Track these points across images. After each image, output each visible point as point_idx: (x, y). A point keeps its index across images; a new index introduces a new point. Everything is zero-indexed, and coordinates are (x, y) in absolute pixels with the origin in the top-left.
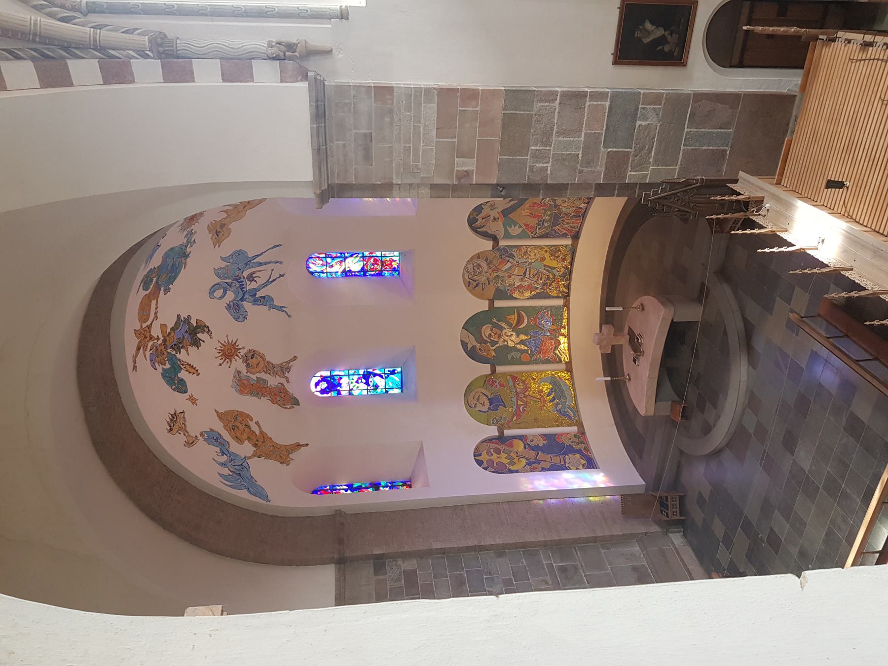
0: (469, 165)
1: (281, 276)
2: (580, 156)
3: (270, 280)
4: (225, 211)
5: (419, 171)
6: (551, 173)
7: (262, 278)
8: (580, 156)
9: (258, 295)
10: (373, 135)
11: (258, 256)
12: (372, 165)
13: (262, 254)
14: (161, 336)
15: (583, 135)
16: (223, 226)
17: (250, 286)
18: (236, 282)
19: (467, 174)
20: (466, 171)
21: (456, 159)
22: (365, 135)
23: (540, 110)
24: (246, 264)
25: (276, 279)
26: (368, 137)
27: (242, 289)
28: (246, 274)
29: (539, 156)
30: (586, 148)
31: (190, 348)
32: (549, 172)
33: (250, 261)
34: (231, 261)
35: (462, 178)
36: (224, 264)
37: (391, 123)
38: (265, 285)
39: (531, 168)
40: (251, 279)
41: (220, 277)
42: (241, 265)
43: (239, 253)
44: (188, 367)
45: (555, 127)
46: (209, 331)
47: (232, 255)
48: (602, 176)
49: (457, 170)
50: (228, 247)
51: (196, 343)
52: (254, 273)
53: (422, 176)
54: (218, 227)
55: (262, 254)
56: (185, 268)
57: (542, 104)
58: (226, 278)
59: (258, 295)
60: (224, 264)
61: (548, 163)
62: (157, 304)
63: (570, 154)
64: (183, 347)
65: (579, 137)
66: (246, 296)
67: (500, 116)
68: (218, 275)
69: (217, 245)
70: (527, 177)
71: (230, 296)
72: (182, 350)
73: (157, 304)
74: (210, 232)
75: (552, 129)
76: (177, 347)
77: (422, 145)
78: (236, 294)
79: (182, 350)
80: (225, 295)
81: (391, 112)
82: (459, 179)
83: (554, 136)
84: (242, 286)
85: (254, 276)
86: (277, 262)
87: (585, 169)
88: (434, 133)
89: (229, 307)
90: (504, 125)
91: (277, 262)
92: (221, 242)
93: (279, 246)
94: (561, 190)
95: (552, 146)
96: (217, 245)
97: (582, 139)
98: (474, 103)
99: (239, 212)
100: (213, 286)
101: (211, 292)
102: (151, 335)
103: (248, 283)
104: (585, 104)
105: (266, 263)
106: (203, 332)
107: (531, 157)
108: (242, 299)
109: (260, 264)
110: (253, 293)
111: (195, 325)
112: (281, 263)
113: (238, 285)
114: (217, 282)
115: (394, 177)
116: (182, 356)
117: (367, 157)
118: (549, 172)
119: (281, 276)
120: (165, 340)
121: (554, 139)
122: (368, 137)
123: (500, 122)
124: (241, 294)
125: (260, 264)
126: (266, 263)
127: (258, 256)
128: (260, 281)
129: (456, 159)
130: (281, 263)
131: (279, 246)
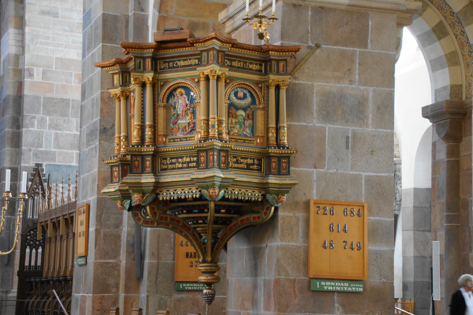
0: (38, 77)
2: (41, 149)
5: (34, 44)
6: (30, 131)
8: (41, 149)
10: (57, 18)
12: (38, 15)
15: (55, 150)
19: (31, 75)
20: (33, 74)
21: (41, 69)
22: (57, 14)
23: (71, 122)
26: (56, 15)
29: (42, 121)
30: (47, 153)
32: (31, 129)
35: (28, 71)
37: (65, 30)
39: (34, 117)
45: (60, 132)
48: (26, 165)
49: (33, 69)
53: (31, 46)
57: (75, 123)
61: (37, 128)
63: (43, 143)
65: (54, 148)
67: (68, 97)
70: (28, 114)
75: (59, 130)
77: (51, 48)
81: (72, 31)
82: (28, 70)
83: (55, 131)
87: (31, 153)
88: (59, 56)
90: (63, 100)
94: (12, 143)
95: (49, 131)
97: (53, 150)
98: (77, 81)
104: (74, 150)
107: (42, 117)
115: (30, 28)
117: (43, 13)
118: (31, 129)
121: (53, 131)
122: (56, 15)
123: (64, 97)
129: (41, 69)
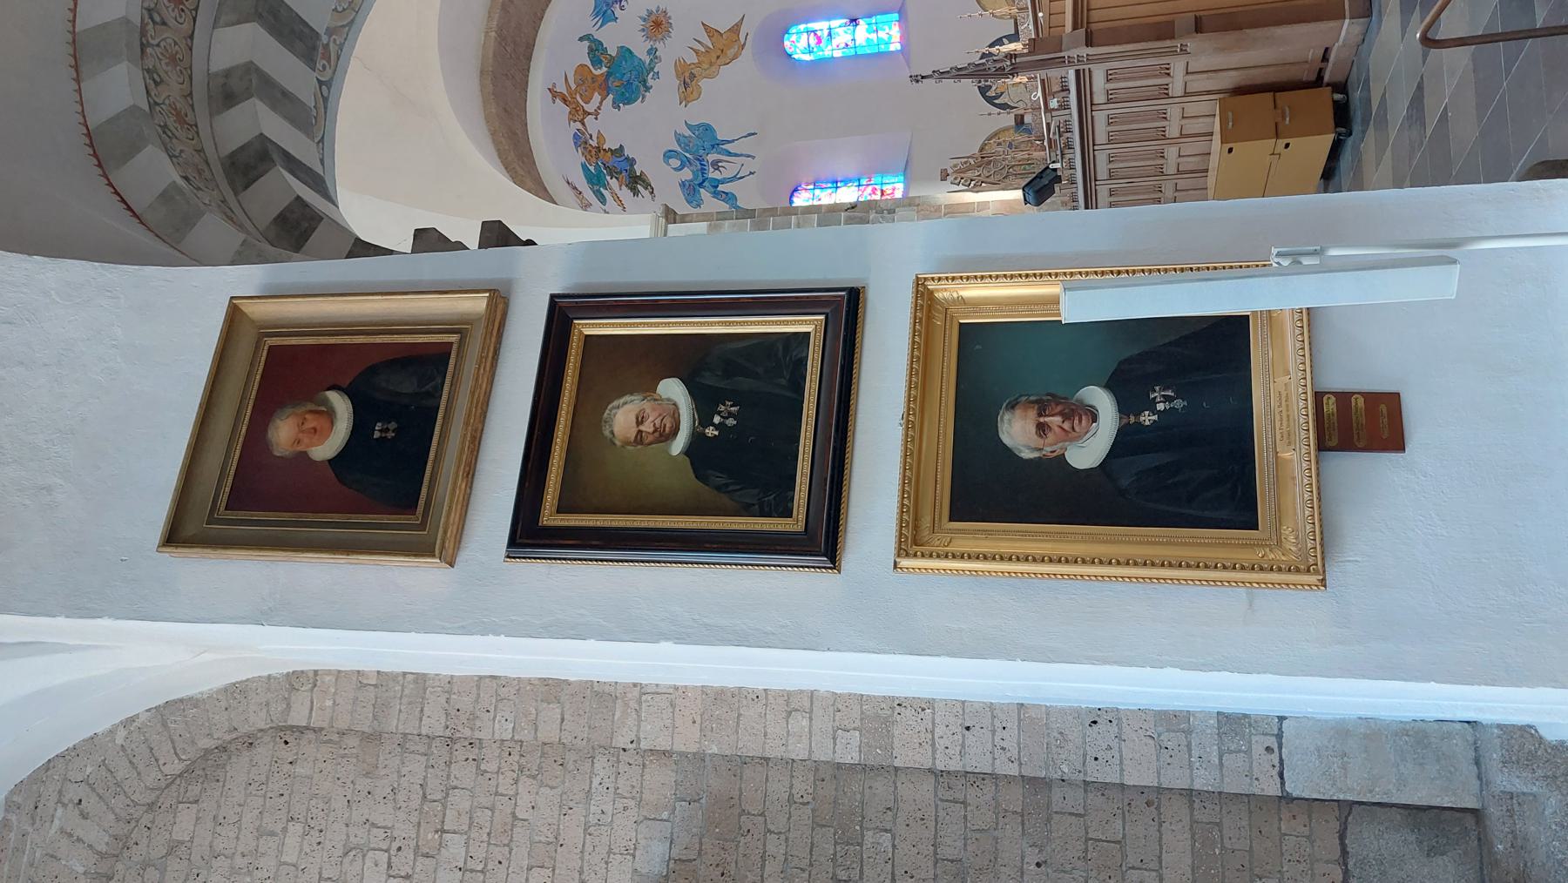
1: (751, 173)
3: (738, 176)
4: (696, 52)
7: (727, 173)
9: (721, 188)
11: (729, 142)
13: (733, 141)
14: (594, 137)
16: (692, 76)
17: (713, 174)
18: (698, 163)
24: (713, 147)
25: (744, 177)
27: (703, 173)
28: (711, 157)
31: (624, 187)
33: (718, 144)
34: (697, 133)
36: (688, 133)
38: (732, 180)
40: (716, 167)
41: (680, 145)
42: (707, 145)
43: (707, 128)
44: (615, 197)
46: (652, 192)
47: (699, 126)
50: (697, 113)
51: (636, 193)
52: (721, 161)
54: (687, 74)
55: (733, 141)
56: (642, 102)
58: (687, 151)
59: (721, 188)
60: (688, 133)
62: (601, 103)
64: (616, 178)
66: (706, 184)
68: (678, 141)
69: (684, 103)
71: (687, 174)
72: (614, 179)
73: (601, 103)
74: (678, 77)
76: (613, 172)
78: (696, 177)
79: (614, 179)
80: (681, 170)
84: (703, 171)
85: (720, 164)
86: (749, 156)
89: (683, 185)
91: (749, 156)
92: (689, 102)
93: (753, 134)
96: (684, 103)
99: (711, 64)
100: (670, 151)
101: (669, 155)
102: (583, 119)
103: (711, 170)
105: (736, 155)
106: (646, 189)
108: (700, 185)
109: (729, 154)
110: (715, 184)
111: (638, 174)
112: (753, 157)
113: (699, 167)
114: (675, 149)
116: (613, 183)
119: (751, 173)
120: (598, 149)
124: (700, 179)
125: (729, 154)
126: (736, 155)
127: (729, 142)
128: (727, 174)
130: (753, 157)
131: (753, 134)
